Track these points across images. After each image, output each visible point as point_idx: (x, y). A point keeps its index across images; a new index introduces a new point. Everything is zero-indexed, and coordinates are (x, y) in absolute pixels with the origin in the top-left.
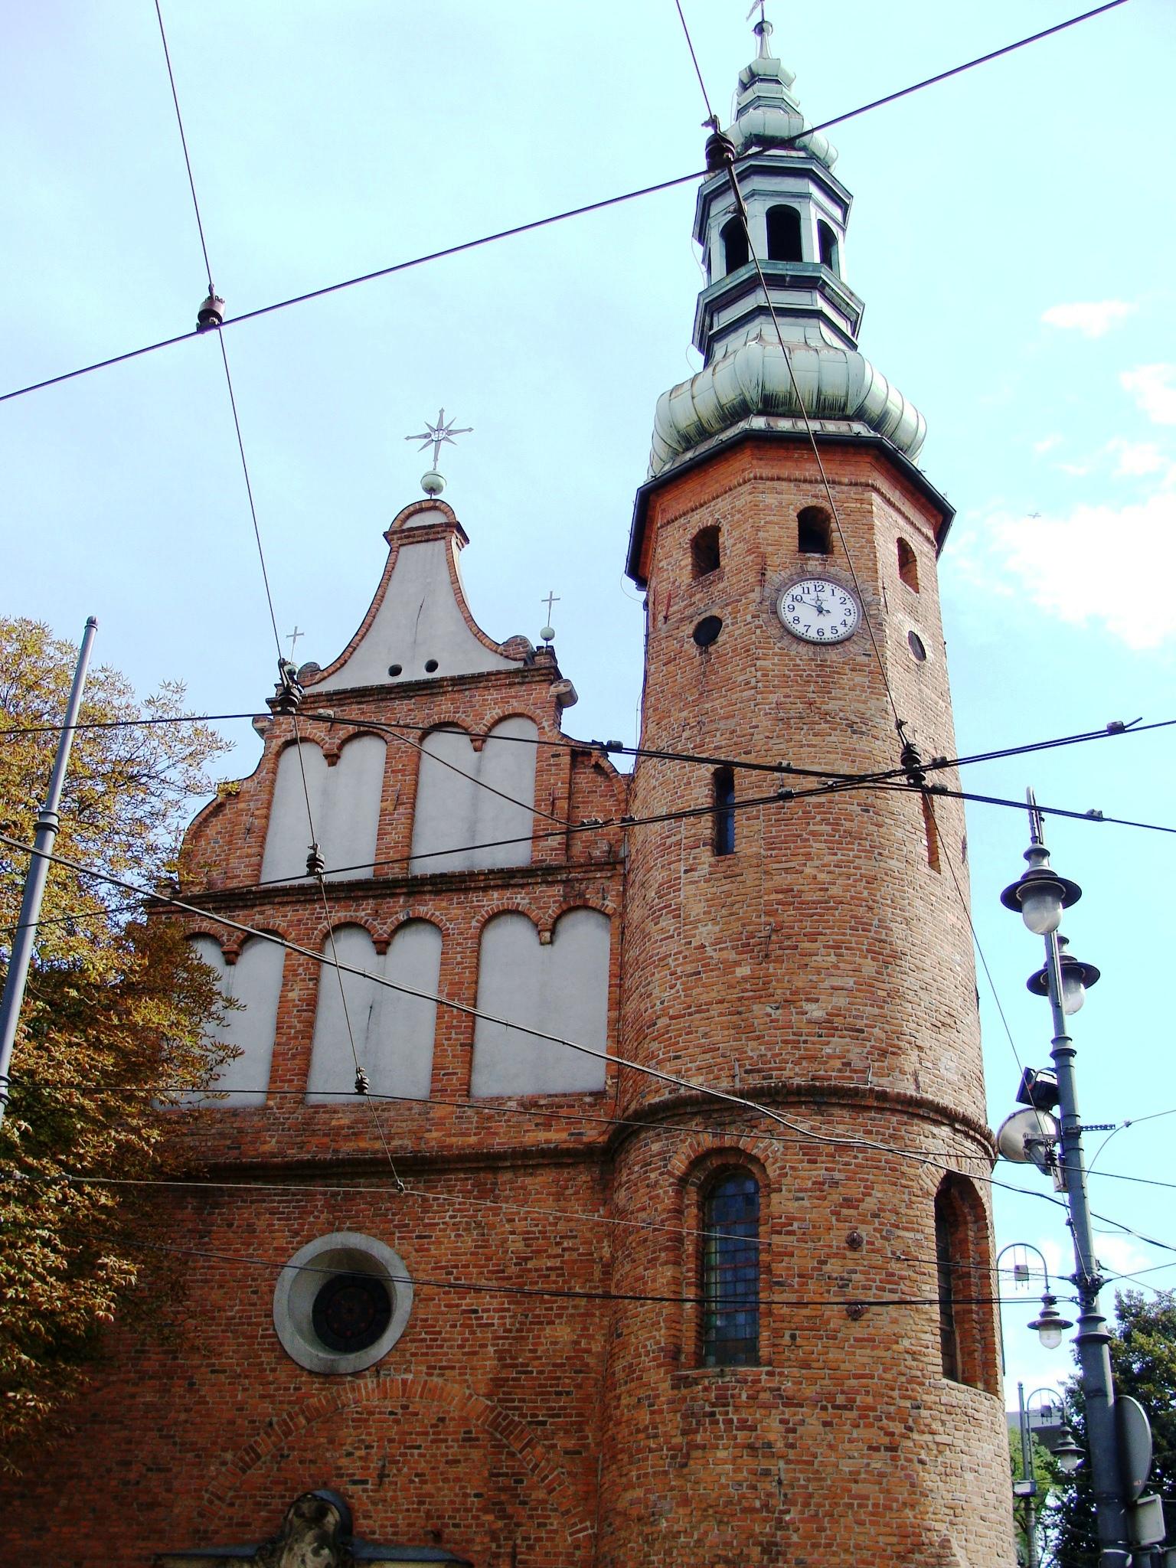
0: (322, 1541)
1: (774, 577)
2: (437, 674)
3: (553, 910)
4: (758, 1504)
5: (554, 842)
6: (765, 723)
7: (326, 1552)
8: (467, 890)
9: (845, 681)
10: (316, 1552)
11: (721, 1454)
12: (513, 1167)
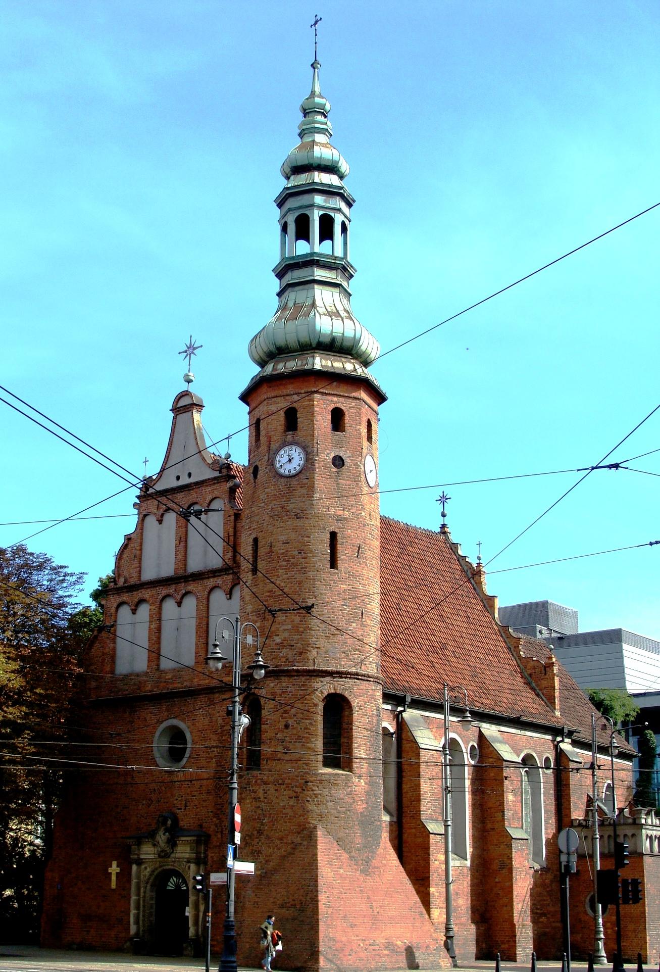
0: (166, 830)
1: (274, 447)
3: (229, 586)
5: (230, 555)
6: (267, 519)
8: (202, 579)
9: (297, 493)
12: (218, 692)
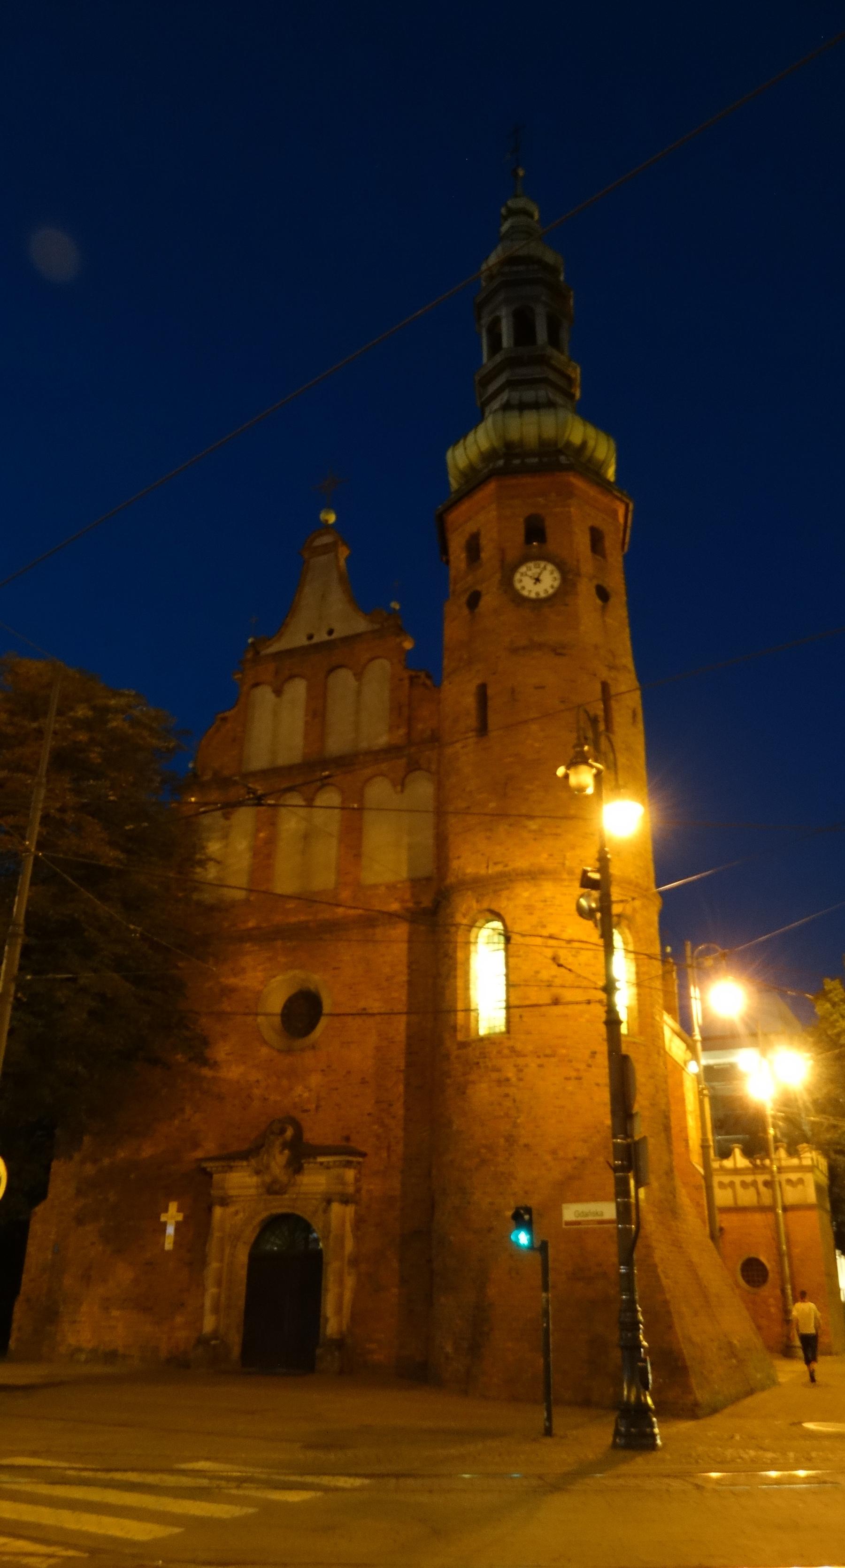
0: (285, 1145)
2: (333, 637)
4: (502, 1114)
5: (402, 731)
7: (286, 1152)
10: (281, 1152)
11: (484, 1086)
